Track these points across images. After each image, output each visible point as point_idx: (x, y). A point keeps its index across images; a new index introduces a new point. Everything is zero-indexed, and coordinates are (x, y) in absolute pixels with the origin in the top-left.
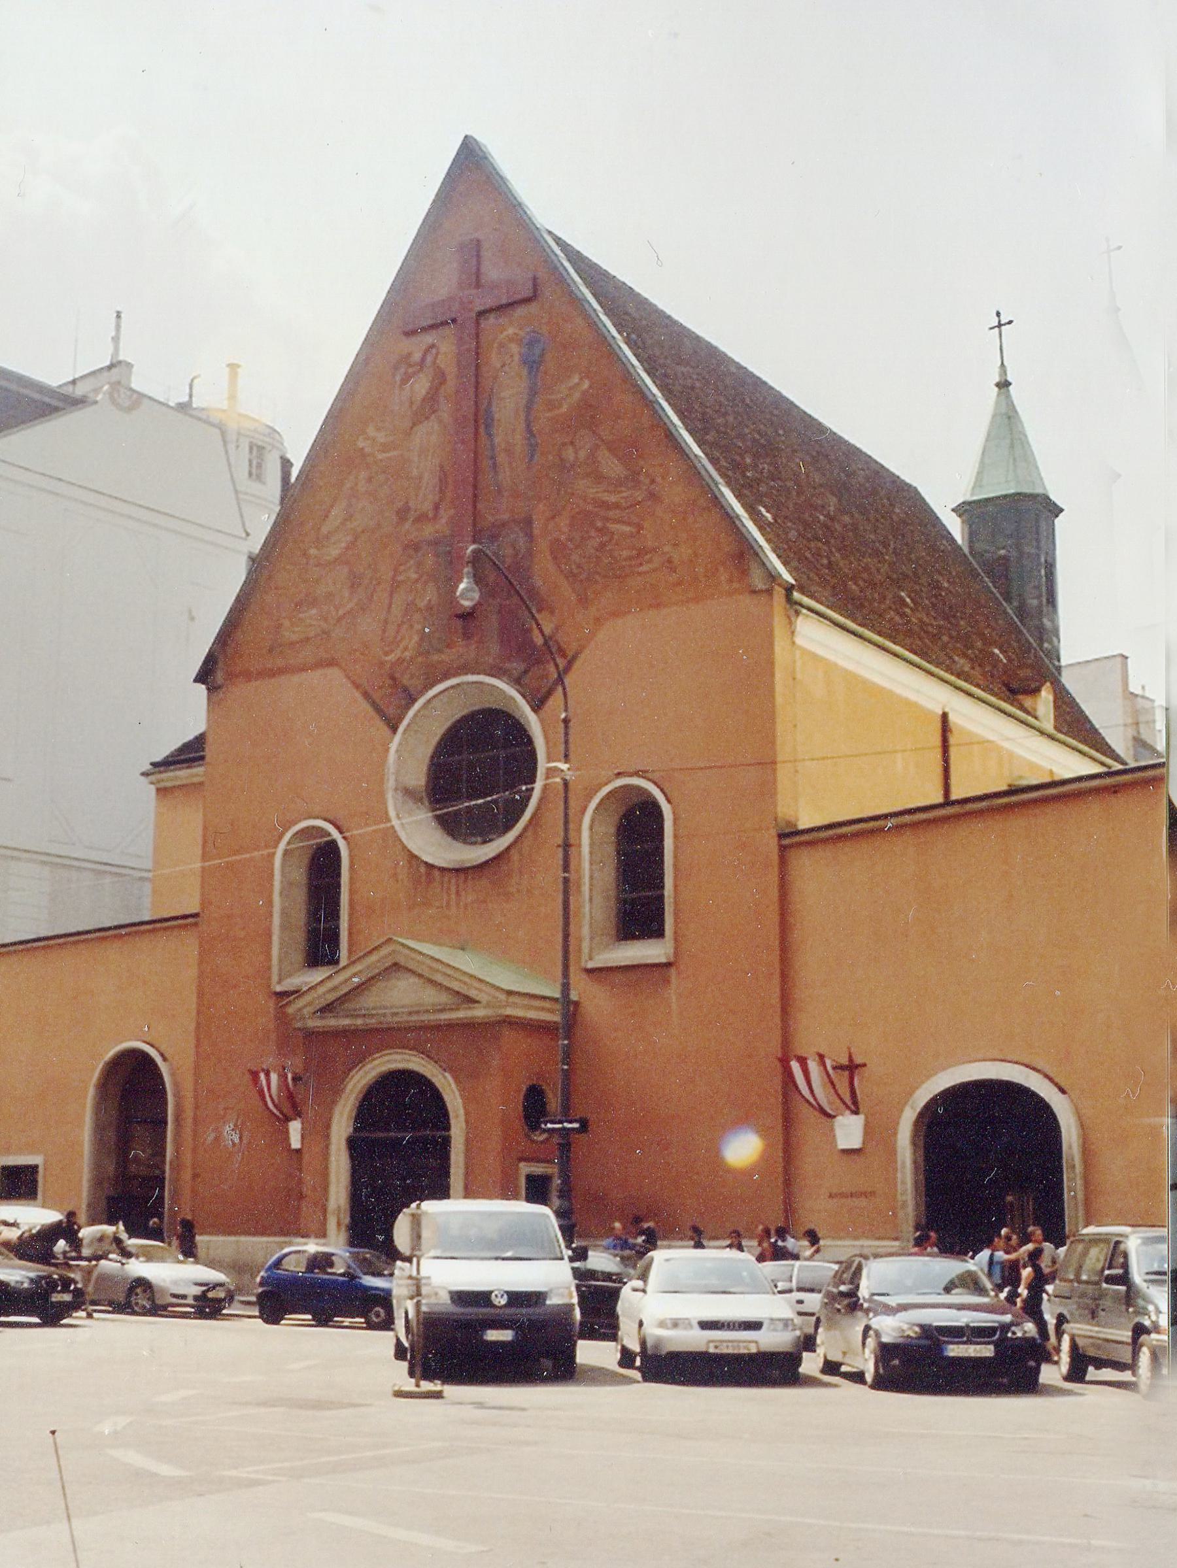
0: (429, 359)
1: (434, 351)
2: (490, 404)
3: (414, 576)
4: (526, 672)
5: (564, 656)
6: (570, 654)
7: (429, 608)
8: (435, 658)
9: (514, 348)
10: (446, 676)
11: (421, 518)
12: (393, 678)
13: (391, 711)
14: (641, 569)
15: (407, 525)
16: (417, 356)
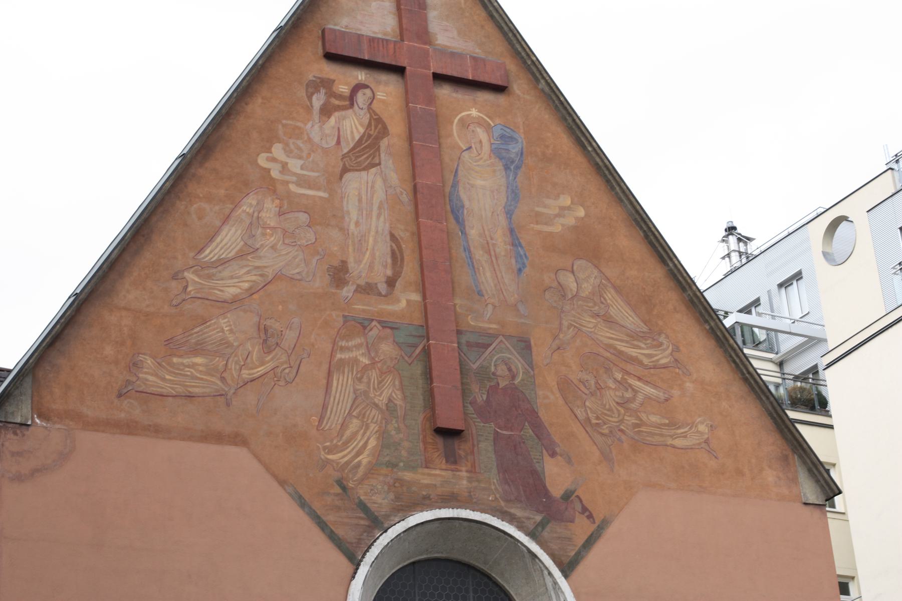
0: (361, 98)
1: (368, 91)
2: (455, 185)
3: (365, 361)
4: (542, 525)
5: (590, 516)
6: (598, 518)
7: (390, 406)
8: (408, 476)
9: (482, 134)
10: (425, 503)
11: (368, 289)
12: (341, 483)
13: (346, 533)
14: (678, 442)
15: (347, 291)
16: (344, 89)
